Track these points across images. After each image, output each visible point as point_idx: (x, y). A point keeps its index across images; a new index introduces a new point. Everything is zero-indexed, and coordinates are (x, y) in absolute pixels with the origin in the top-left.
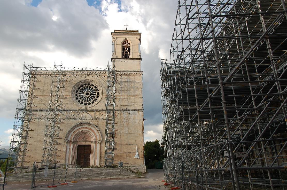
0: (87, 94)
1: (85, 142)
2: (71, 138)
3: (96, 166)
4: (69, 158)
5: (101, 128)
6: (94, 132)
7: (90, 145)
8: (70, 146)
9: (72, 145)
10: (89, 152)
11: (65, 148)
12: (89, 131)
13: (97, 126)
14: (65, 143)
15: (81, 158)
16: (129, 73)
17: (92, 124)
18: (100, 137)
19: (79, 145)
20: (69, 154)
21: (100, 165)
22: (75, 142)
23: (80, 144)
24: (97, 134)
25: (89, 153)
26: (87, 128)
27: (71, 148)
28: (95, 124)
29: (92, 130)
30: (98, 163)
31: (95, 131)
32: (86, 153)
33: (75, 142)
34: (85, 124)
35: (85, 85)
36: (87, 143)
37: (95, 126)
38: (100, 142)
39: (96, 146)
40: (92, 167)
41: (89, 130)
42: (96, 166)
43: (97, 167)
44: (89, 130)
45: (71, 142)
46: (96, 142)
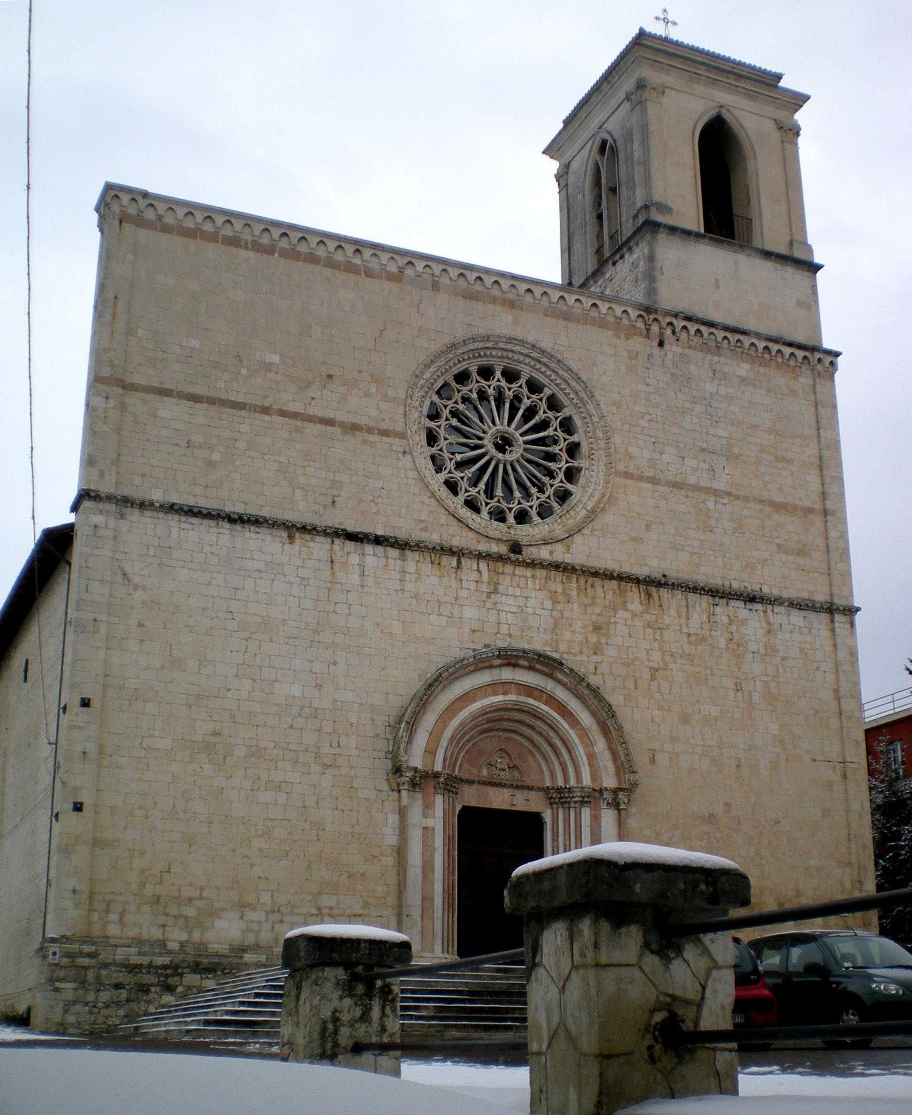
0: (504, 443)
1: (506, 793)
2: (431, 752)
4: (427, 899)
6: (574, 722)
8: (428, 806)
11: (393, 819)
16: (761, 345)
23: (474, 803)
34: (522, 662)
35: (486, 373)
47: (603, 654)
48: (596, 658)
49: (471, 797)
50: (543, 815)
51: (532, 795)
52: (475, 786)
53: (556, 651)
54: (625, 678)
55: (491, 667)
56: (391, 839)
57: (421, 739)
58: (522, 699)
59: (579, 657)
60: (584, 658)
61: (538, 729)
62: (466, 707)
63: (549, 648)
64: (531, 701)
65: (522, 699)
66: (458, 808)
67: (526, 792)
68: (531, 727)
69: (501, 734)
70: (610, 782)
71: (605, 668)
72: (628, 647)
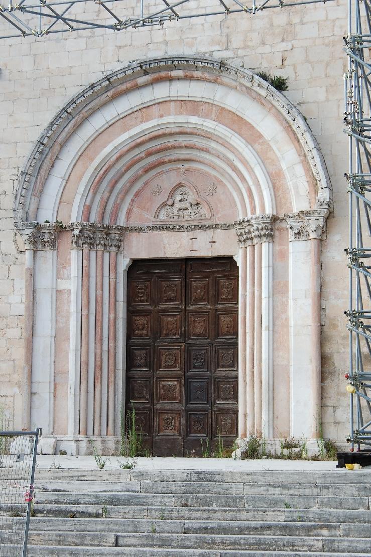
1: (185, 236)
3: (292, 450)
5: (321, 96)
6: (253, 136)
7: (229, 261)
9: (74, 256)
10: (225, 320)
11: (21, 285)
12: (207, 136)
13: (280, 85)
14: (20, 240)
15: (161, 372)
17: (235, 63)
18: (314, 182)
19: (137, 266)
20: (59, 337)
21: (321, 434)
22: (98, 235)
23: (144, 255)
24: (287, 157)
25: (225, 330)
26: (193, 106)
27: (71, 284)
28: (265, 67)
29: (237, 122)
30: (302, 424)
31: (268, 126)
32: (199, 330)
33: (98, 235)
34: (174, 73)
36: (204, 246)
37: (264, 77)
38: (312, 225)
39: (280, 257)
40: (252, 453)
41: (209, 125)
42: (288, 446)
43: (298, 457)
44: (222, 130)
45: (67, 240)
46: (273, 227)
47: (295, 39)
48: (286, 46)
49: (142, 247)
50: (235, 258)
51: (219, 235)
52: (146, 234)
53: (227, 49)
54: (328, 64)
55: (138, 87)
56: (20, 308)
57: (54, 185)
58: (181, 119)
59: (260, 50)
60: (267, 49)
61: (214, 152)
62: (111, 141)
63: (217, 48)
64: (194, 119)
65: (181, 119)
66: (124, 263)
67: (210, 231)
68: (206, 151)
69: (179, 166)
70: (298, 204)
71: (297, 56)
72: (334, 21)
